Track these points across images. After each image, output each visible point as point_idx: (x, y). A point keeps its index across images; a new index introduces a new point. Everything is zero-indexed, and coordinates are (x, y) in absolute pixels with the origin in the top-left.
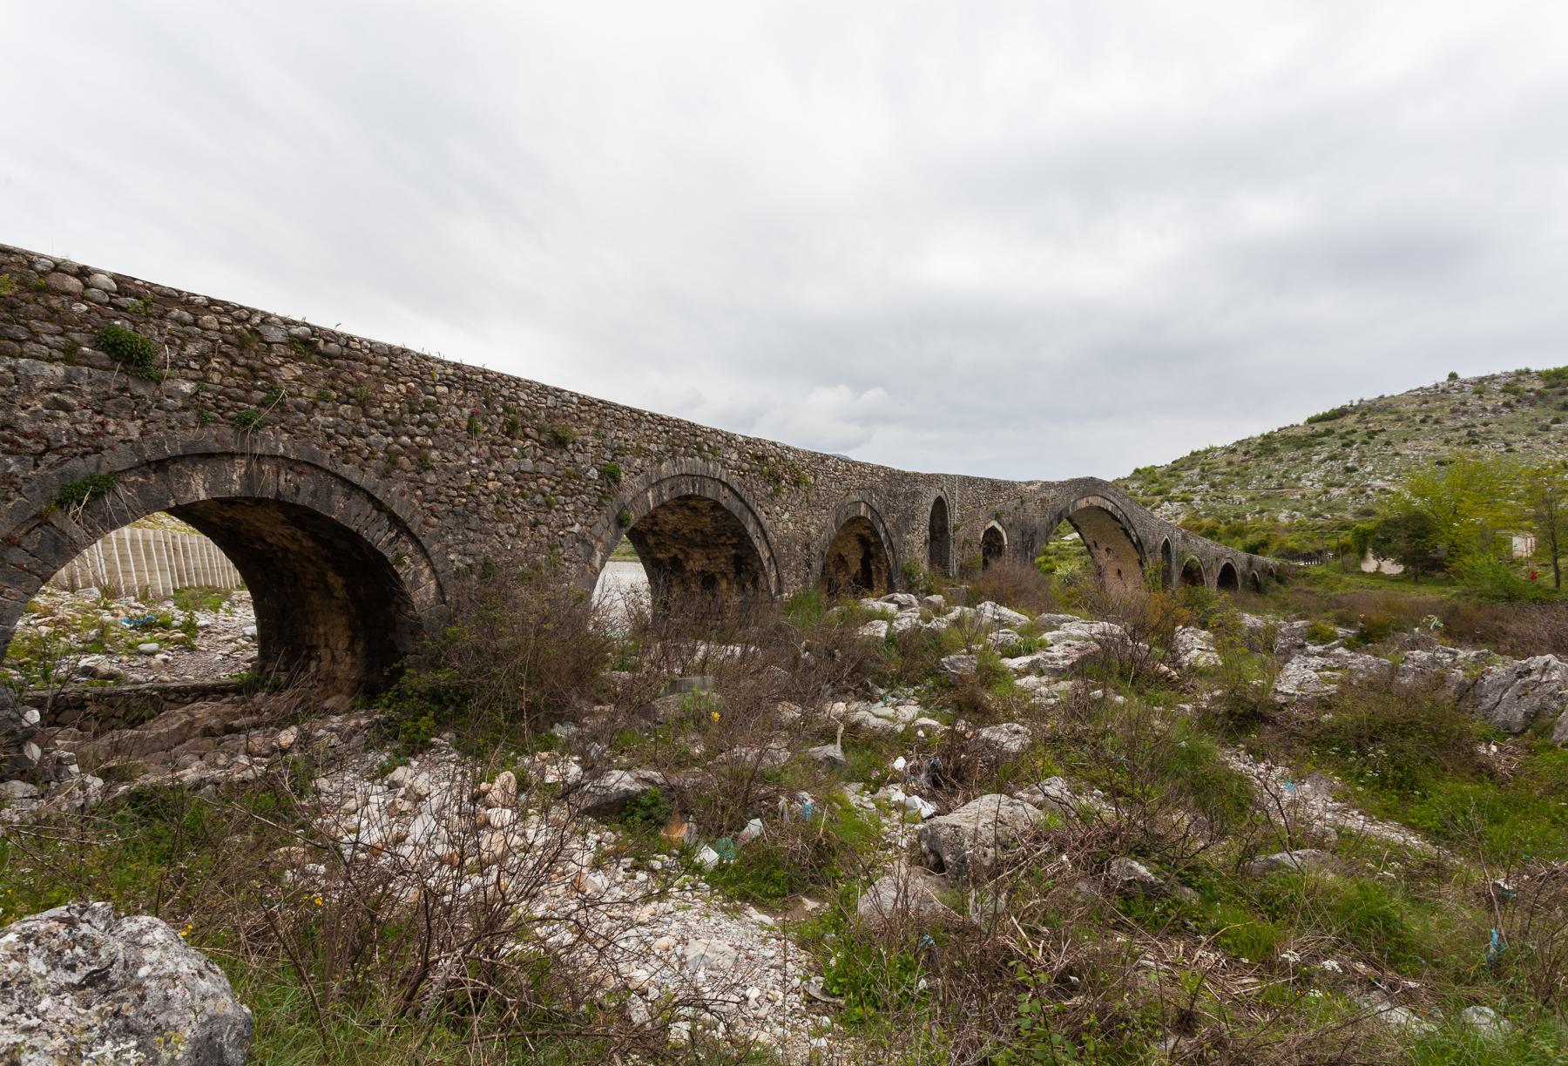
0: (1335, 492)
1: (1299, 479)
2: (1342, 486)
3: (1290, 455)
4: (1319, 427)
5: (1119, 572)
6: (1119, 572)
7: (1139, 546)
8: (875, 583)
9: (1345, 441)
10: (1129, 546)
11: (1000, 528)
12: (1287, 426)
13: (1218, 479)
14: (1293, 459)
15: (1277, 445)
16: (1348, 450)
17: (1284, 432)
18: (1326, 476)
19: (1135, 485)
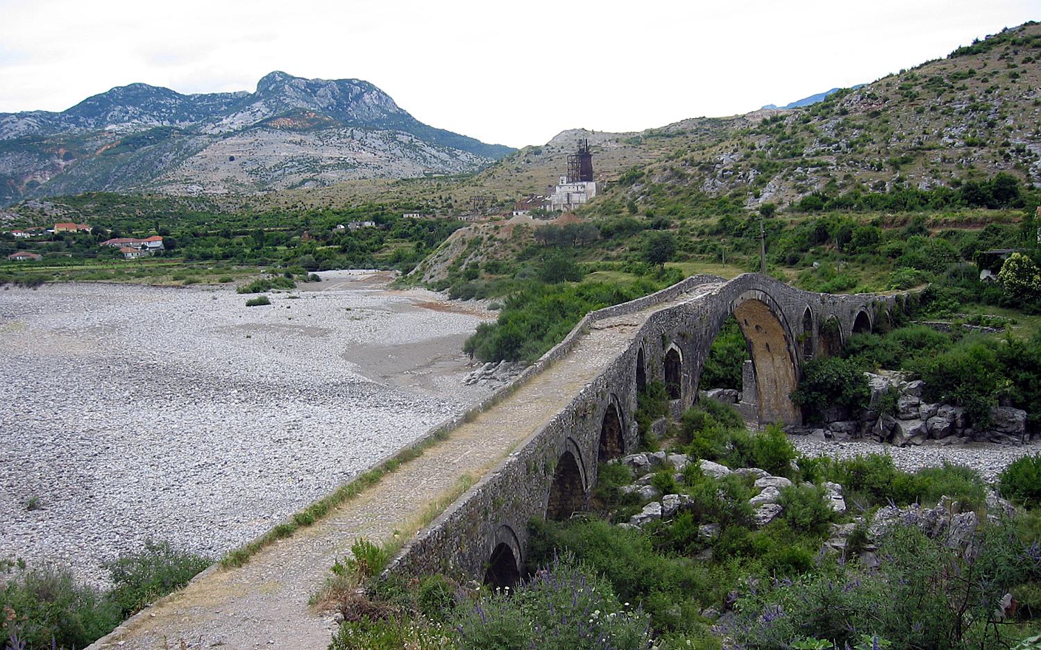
0: (977, 153)
1: (940, 136)
2: (983, 145)
3: (931, 103)
4: (964, 65)
5: (767, 345)
6: (767, 345)
7: (785, 323)
8: (608, 440)
9: (988, 86)
10: (776, 324)
11: (676, 348)
12: (930, 60)
13: (855, 135)
14: (934, 109)
15: (918, 89)
16: (989, 96)
17: (923, 71)
18: (967, 132)
19: (763, 143)
